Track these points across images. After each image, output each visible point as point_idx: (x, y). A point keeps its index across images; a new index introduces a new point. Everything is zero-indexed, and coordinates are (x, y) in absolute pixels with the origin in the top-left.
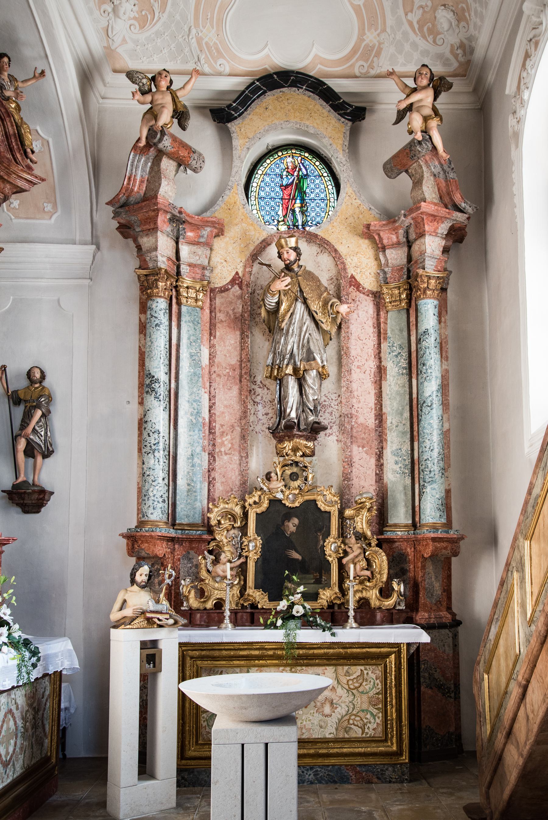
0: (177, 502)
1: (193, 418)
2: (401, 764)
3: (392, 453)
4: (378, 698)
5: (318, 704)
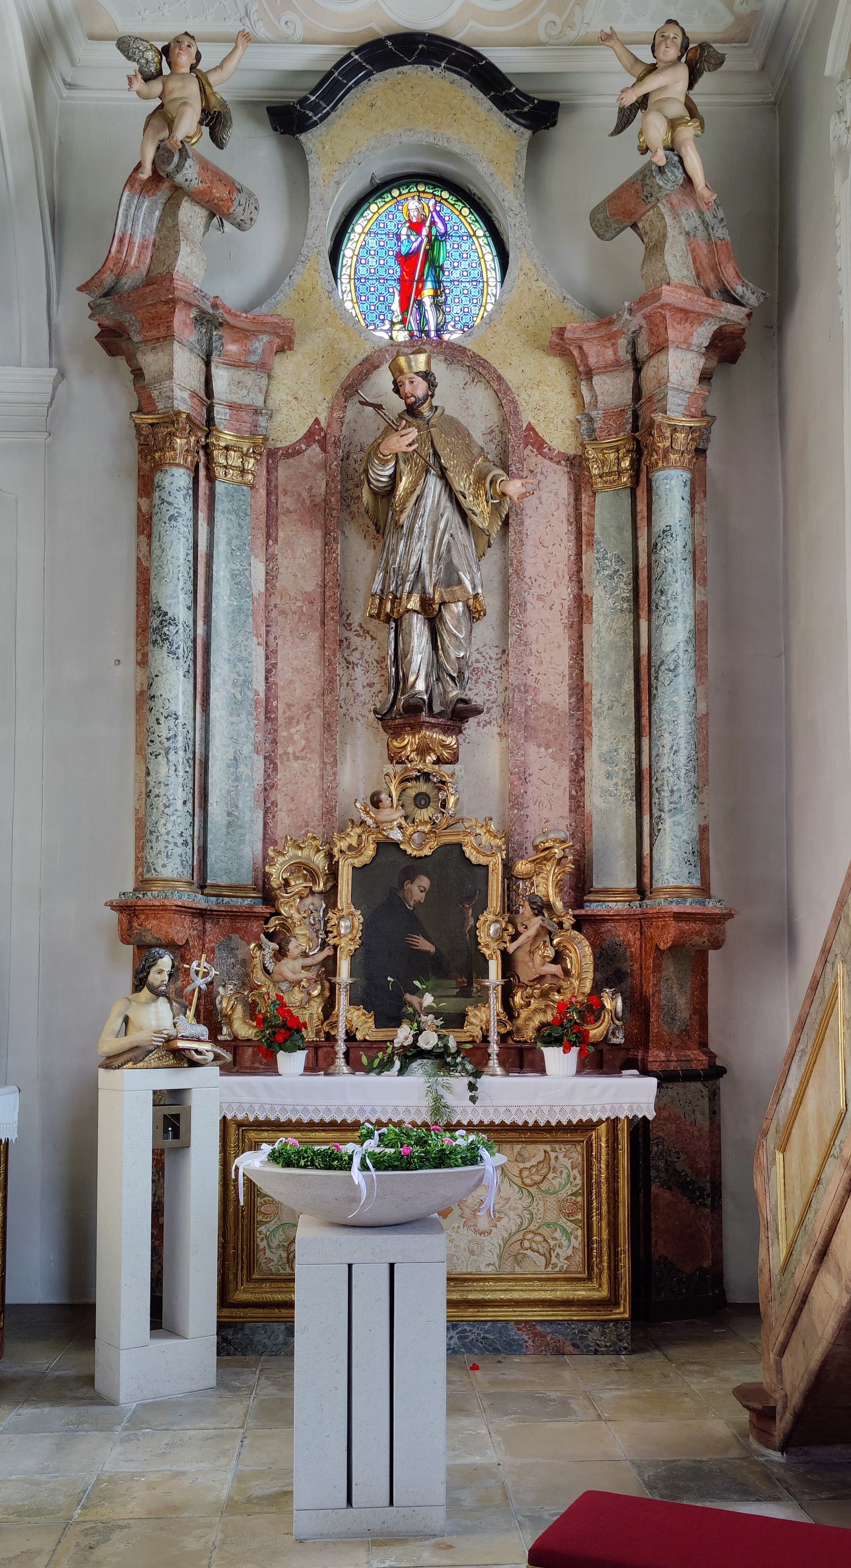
0: (209, 846)
1: (236, 691)
2: (616, 1321)
3: (600, 756)
4: (575, 1203)
5: (467, 1212)
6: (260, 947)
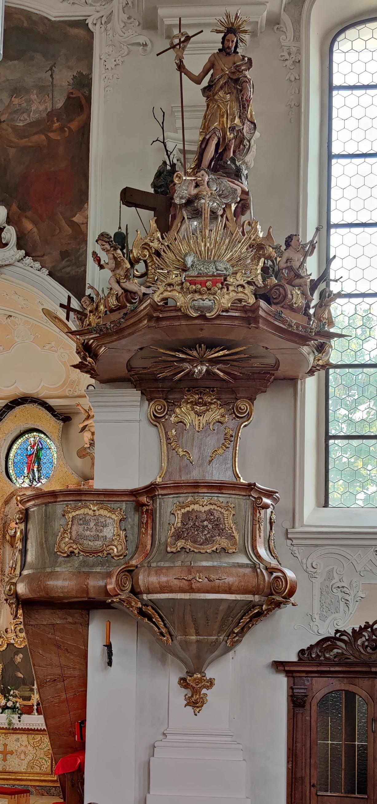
4: (49, 752)
5: (18, 753)
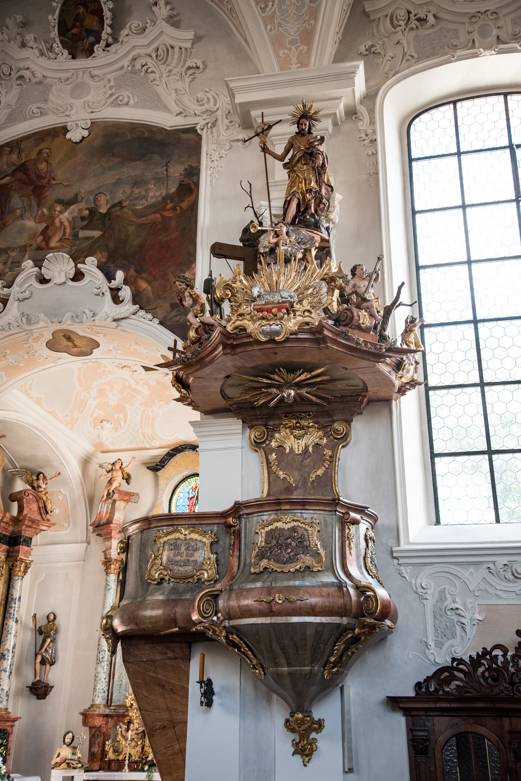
6: (120, 727)
